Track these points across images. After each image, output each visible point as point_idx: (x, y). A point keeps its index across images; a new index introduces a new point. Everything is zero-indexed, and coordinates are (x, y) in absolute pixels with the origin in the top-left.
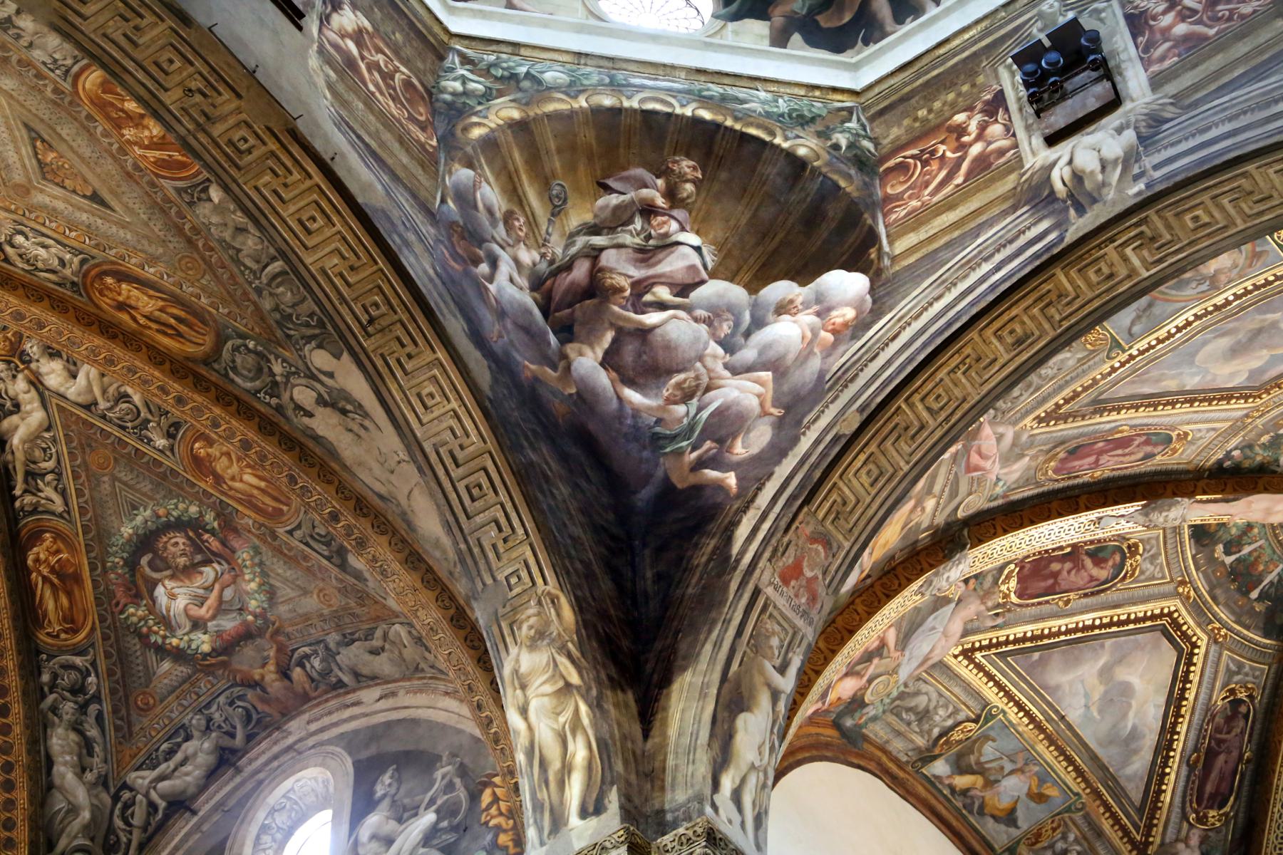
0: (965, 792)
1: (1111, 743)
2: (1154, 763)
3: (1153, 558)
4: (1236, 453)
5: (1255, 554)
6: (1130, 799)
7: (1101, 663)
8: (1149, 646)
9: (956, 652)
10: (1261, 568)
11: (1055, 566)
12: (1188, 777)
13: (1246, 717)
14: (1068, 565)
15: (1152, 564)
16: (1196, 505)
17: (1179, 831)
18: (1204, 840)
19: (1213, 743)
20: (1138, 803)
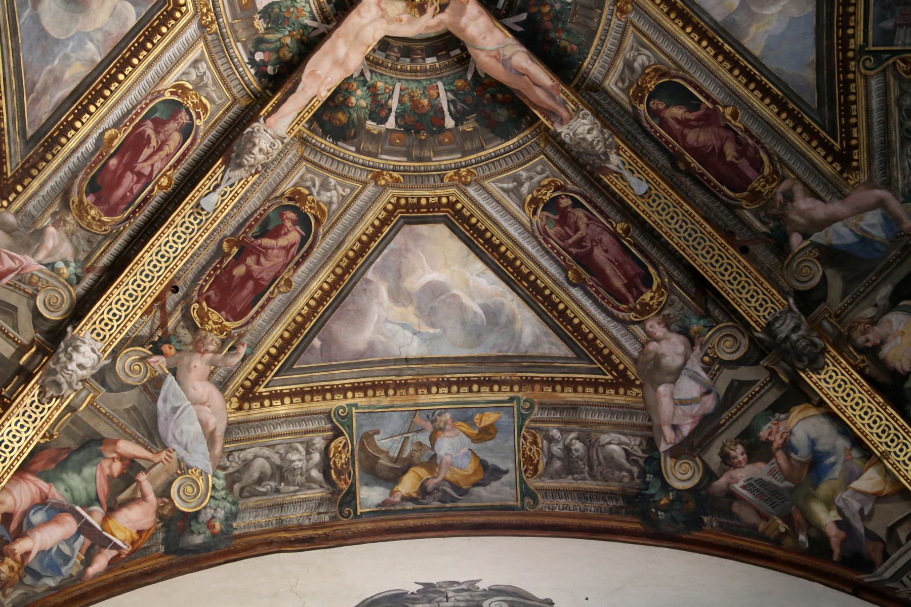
0: (423, 491)
1: (479, 336)
2: (540, 314)
3: (325, 186)
4: (259, 56)
5: (406, 98)
6: (560, 358)
7: (383, 291)
8: (411, 244)
9: (235, 405)
10: (425, 102)
11: (239, 271)
12: (587, 293)
13: (576, 204)
14: (250, 260)
15: (329, 190)
16: (270, 120)
17: (636, 338)
18: (667, 323)
19: (574, 251)
20: (571, 354)
